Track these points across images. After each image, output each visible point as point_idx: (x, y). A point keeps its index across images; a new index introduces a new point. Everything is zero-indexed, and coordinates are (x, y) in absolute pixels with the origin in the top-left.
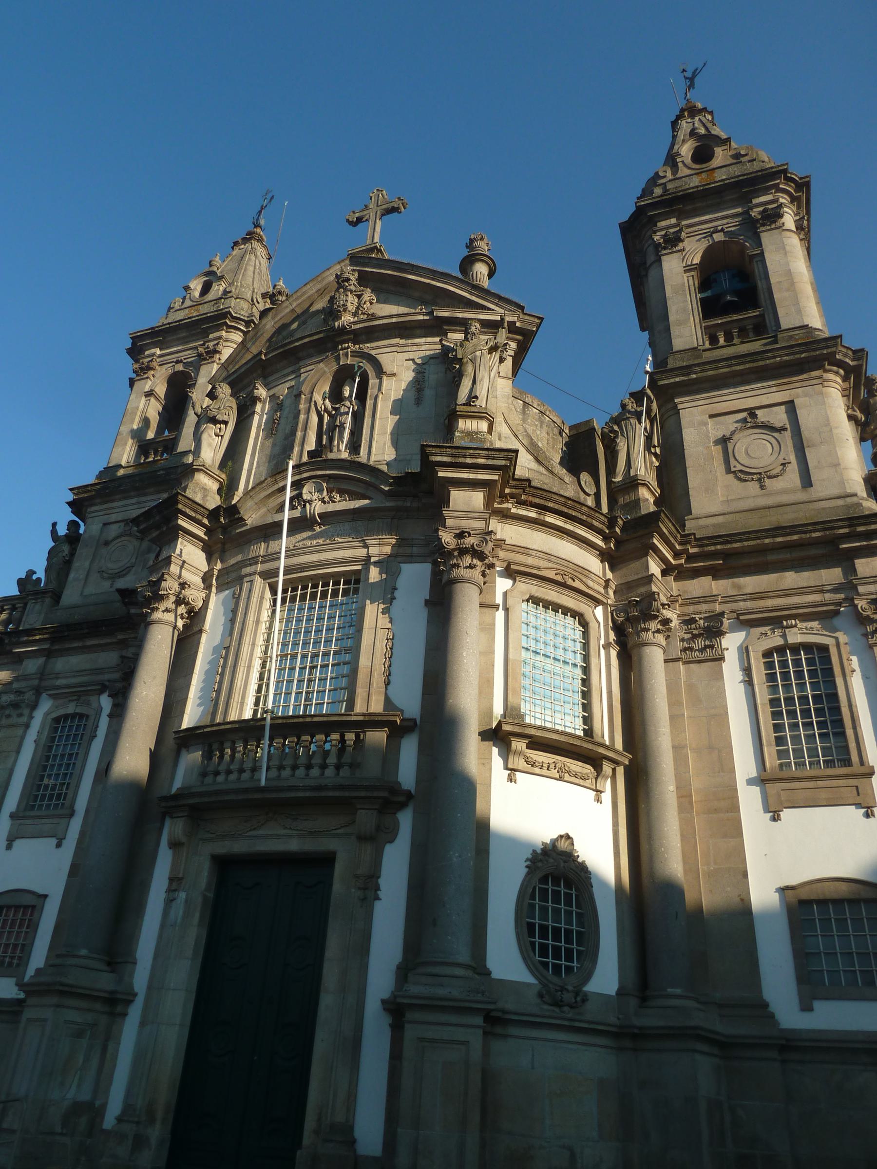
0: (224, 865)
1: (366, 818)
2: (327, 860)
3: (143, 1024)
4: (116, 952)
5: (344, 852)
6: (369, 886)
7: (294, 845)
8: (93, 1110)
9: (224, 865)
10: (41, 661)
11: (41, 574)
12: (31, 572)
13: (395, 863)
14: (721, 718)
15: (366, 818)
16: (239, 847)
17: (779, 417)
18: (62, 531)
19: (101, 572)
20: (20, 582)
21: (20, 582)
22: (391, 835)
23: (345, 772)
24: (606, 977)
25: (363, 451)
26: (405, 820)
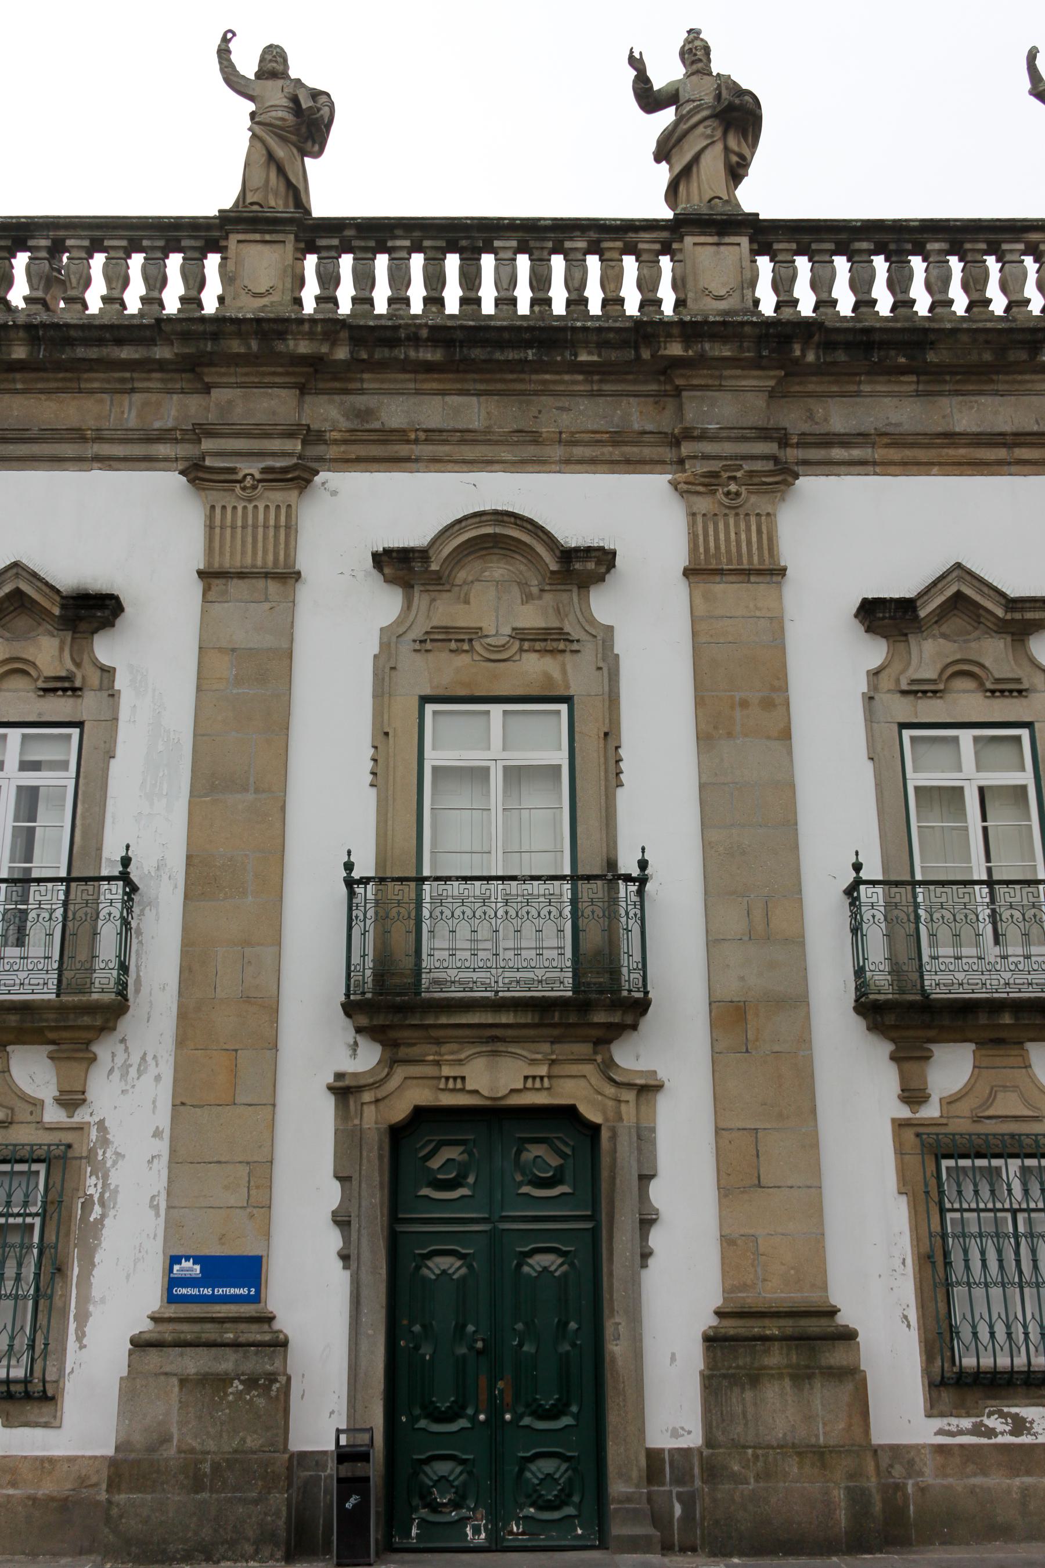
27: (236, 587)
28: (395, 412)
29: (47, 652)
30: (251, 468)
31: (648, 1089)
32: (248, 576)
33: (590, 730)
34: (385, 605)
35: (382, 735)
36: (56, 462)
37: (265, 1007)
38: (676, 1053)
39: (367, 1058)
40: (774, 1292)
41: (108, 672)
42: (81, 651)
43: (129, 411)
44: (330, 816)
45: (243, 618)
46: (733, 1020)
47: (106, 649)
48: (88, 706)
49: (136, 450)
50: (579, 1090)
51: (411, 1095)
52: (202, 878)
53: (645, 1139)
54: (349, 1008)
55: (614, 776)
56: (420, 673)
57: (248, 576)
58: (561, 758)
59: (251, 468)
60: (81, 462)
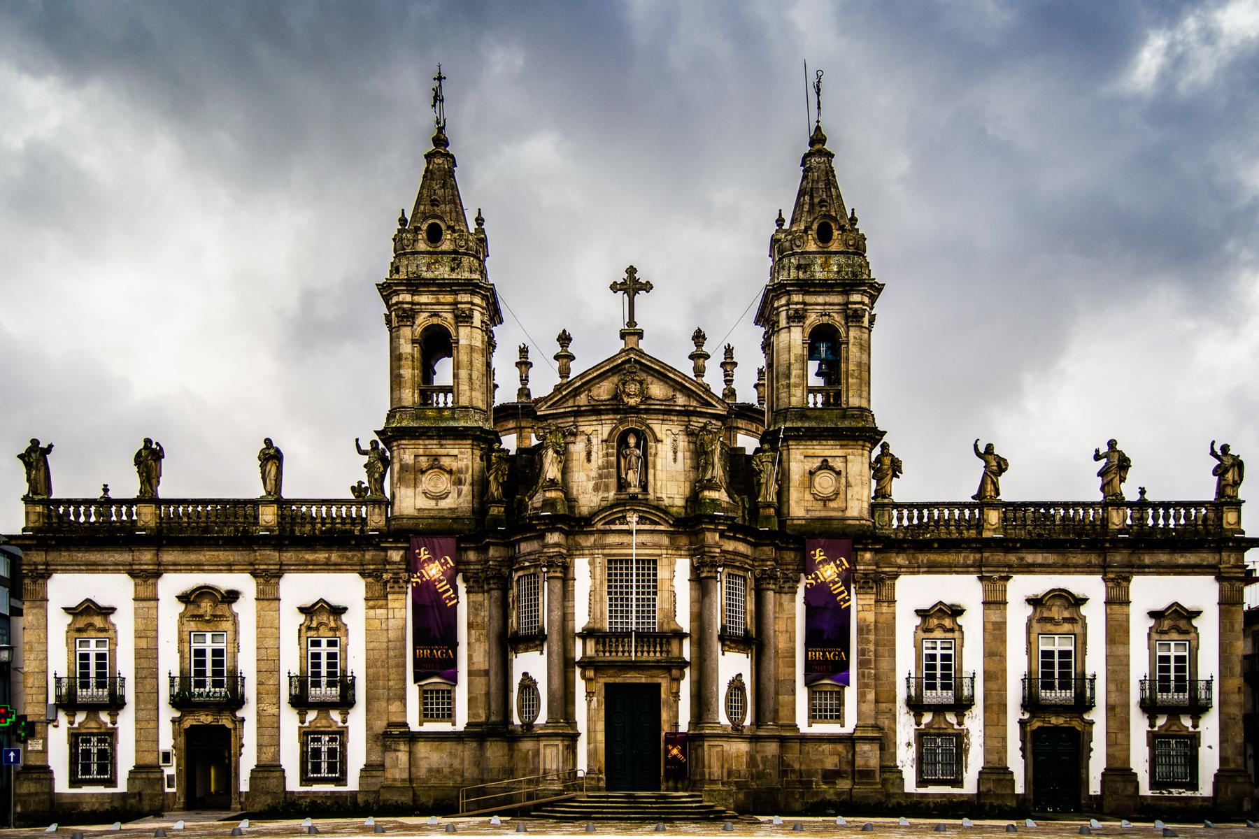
0: (606, 684)
1: (675, 672)
2: (659, 685)
3: (589, 743)
4: (570, 719)
5: (664, 684)
6: (676, 695)
7: (643, 680)
8: (574, 772)
9: (606, 684)
10: (401, 552)
11: (367, 484)
12: (360, 483)
13: (685, 687)
14: (792, 618)
15: (675, 672)
16: (618, 680)
17: (838, 464)
18: (366, 446)
19: (425, 493)
20: (353, 489)
21: (353, 489)
22: (682, 676)
23: (664, 655)
24: (747, 722)
25: (650, 490)
26: (687, 671)
27: (993, 606)
28: (1030, 558)
29: (947, 623)
30: (996, 576)
31: (1091, 723)
32: (995, 602)
33: (1080, 642)
34: (1029, 610)
35: (1029, 643)
36: (944, 573)
37: (1003, 707)
38: (1098, 716)
39: (1027, 716)
40: (1118, 765)
41: (961, 627)
42: (954, 621)
43: (960, 558)
44: (1017, 665)
45: (994, 616)
46: (1110, 708)
47: (960, 620)
48: (957, 634)
49: (964, 569)
50: (1076, 724)
51: (1037, 724)
52: (988, 676)
53: (1090, 734)
54: (1022, 706)
55: (1084, 653)
56: (1036, 627)
57: (995, 602)
58: (1072, 648)
59: (996, 576)
60: (950, 573)
